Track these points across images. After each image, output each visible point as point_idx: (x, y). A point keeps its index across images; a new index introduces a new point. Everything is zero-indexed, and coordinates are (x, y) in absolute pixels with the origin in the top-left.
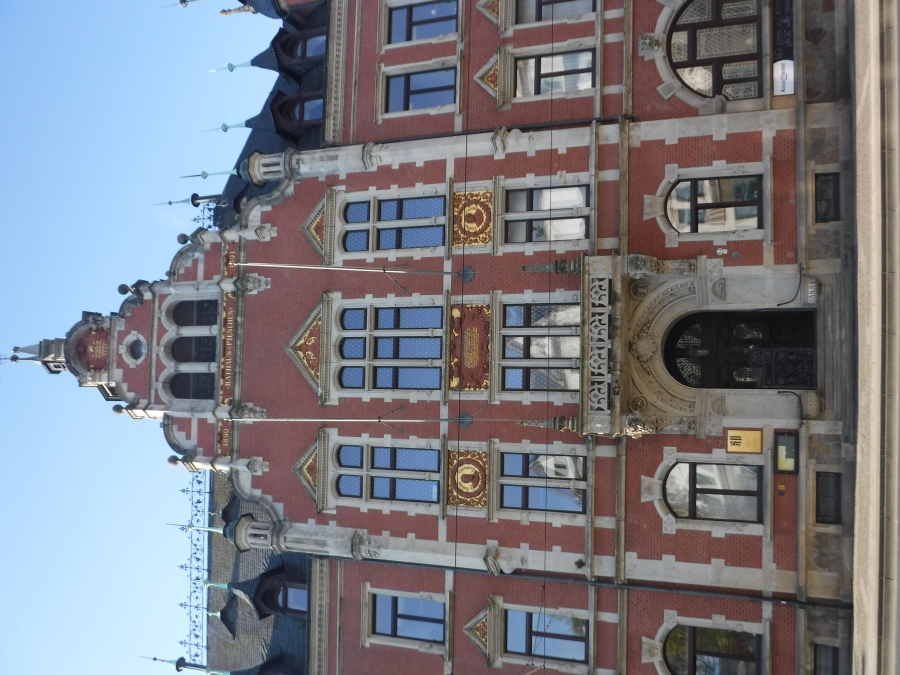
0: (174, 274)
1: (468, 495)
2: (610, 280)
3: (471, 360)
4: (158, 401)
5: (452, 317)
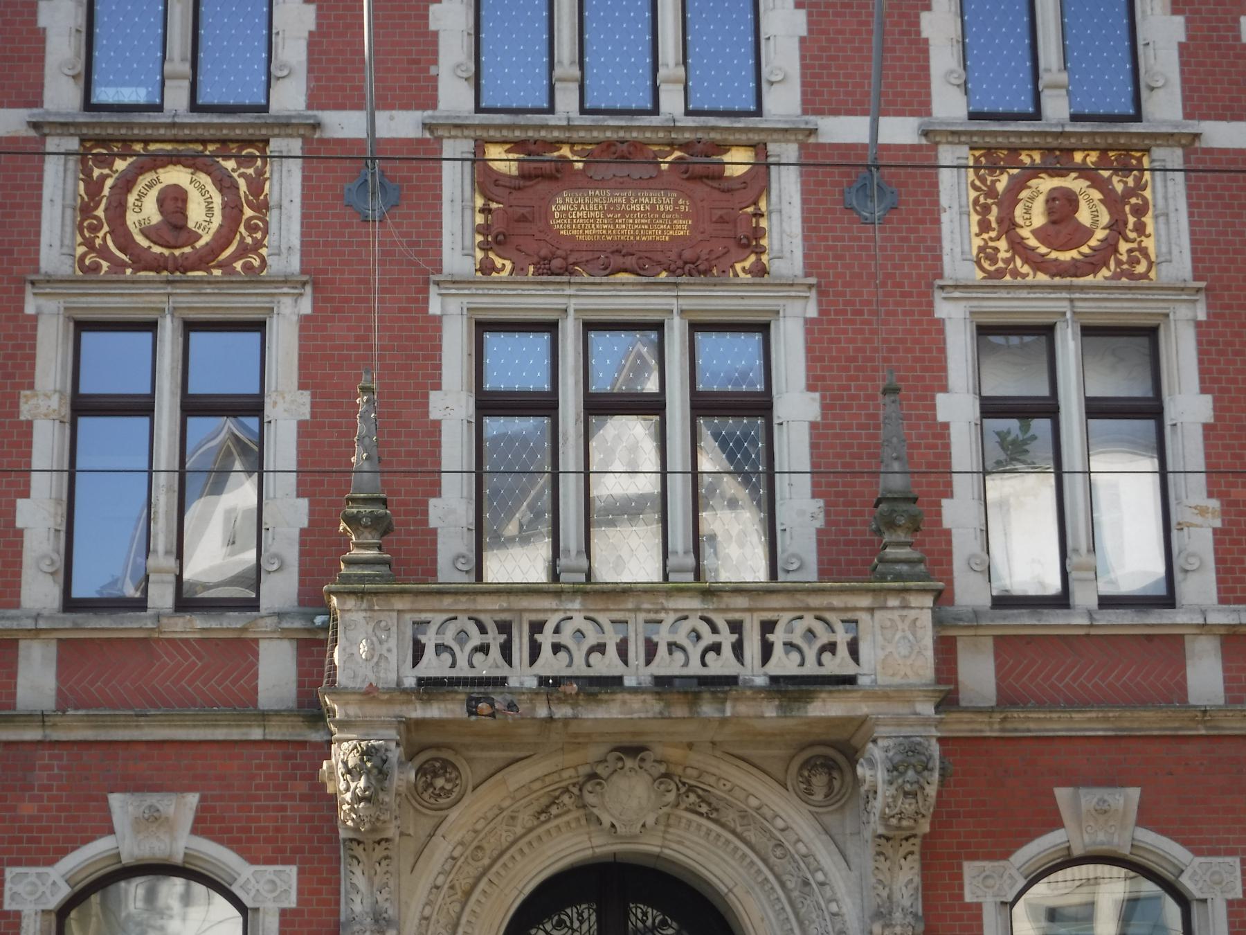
1: (118, 210)
2: (850, 680)
5: (723, 148)
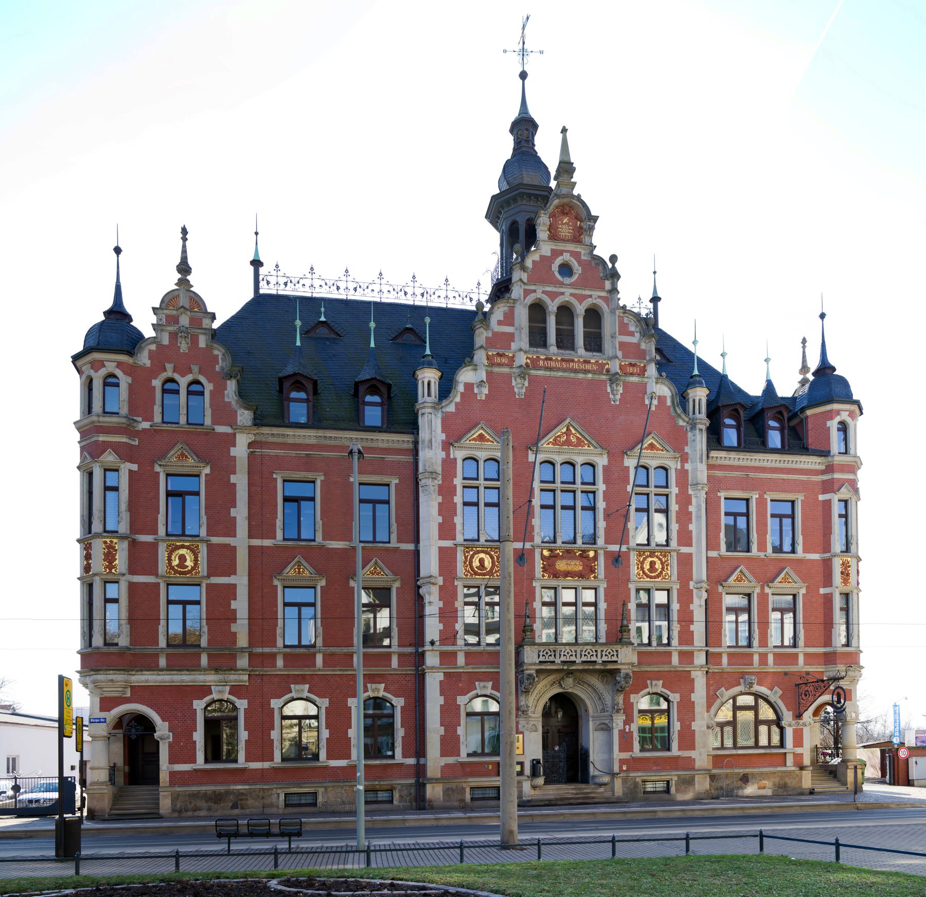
0: (624, 313)
1: (471, 563)
2: (616, 662)
3: (561, 565)
4: (527, 293)
5: (589, 551)
